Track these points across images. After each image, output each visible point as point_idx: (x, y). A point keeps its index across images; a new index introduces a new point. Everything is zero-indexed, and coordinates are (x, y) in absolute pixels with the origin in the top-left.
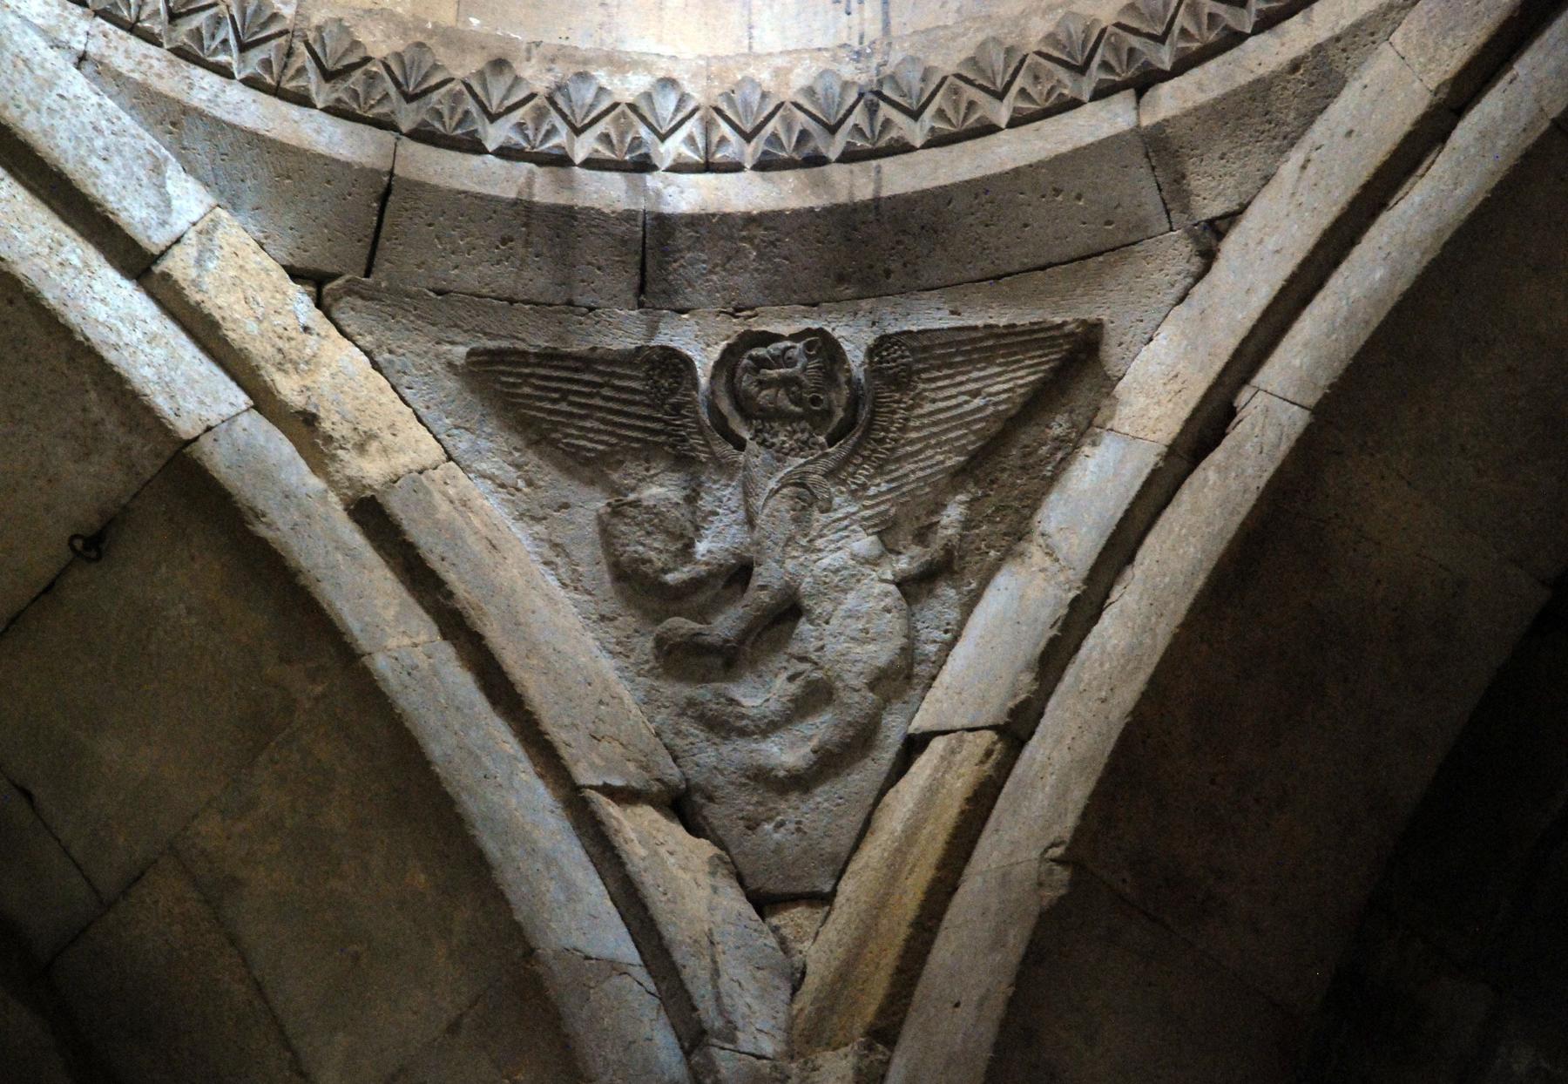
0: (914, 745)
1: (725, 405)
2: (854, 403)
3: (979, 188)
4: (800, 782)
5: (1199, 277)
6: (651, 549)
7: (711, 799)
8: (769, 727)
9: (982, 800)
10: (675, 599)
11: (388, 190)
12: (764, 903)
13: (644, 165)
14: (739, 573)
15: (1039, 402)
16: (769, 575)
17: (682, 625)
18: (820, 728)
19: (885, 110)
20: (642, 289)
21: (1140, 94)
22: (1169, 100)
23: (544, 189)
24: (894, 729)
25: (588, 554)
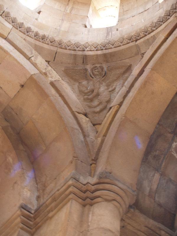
0: (111, 108)
1: (91, 74)
2: (105, 73)
3: (119, 51)
5: (142, 59)
6: (84, 89)
7: (89, 114)
8: (95, 107)
9: (117, 112)
10: (86, 94)
11: (56, 53)
12: (94, 125)
13: (84, 51)
14: (93, 91)
15: (124, 73)
16: (95, 91)
17: (86, 97)
19: (109, 44)
20: (83, 63)
21: (136, 41)
22: (138, 42)
23: (73, 52)
24: (109, 107)
25: (77, 90)
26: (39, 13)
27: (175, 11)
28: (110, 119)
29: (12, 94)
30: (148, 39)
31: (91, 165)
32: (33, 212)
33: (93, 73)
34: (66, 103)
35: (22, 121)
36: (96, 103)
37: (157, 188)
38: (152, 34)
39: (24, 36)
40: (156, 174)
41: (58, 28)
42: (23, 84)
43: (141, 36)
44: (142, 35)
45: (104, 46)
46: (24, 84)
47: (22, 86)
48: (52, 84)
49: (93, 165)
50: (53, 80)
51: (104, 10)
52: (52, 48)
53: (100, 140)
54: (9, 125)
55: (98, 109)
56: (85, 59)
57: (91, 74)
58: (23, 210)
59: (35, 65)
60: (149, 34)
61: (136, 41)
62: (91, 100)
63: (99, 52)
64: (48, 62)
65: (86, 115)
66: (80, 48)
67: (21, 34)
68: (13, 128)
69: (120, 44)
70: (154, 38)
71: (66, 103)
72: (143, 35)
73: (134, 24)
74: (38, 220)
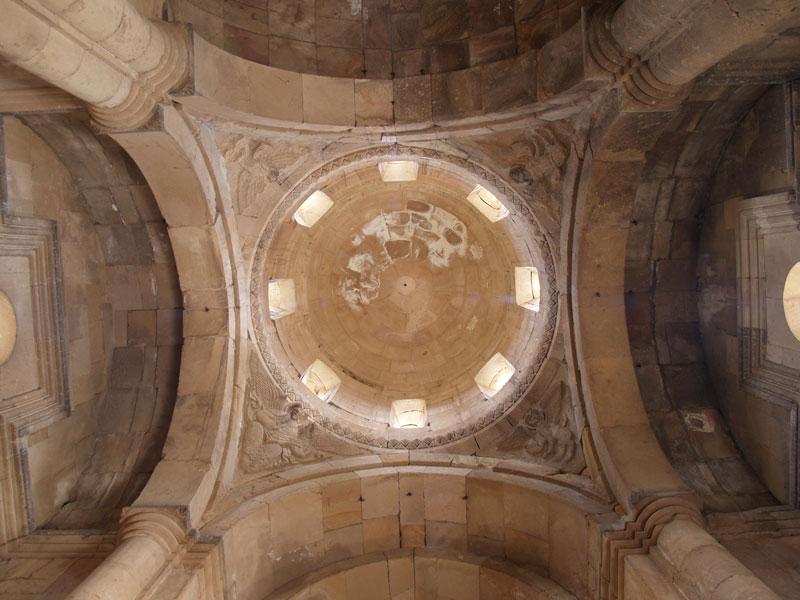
0: (581, 441)
2: (544, 414)
3: (537, 382)
4: (573, 457)
6: (535, 449)
8: (565, 454)
9: (590, 435)
10: (541, 452)
12: (580, 474)
15: (563, 394)
17: (545, 454)
18: (570, 449)
23: (493, 424)
24: (578, 442)
25: (528, 456)
26: (429, 425)
28: (591, 453)
30: (556, 342)
31: (614, 509)
33: (531, 425)
36: (561, 451)
37: (716, 479)
39: (428, 450)
40: (700, 466)
44: (546, 346)
45: (520, 392)
47: (466, 498)
50: (494, 465)
52: (467, 439)
53: (599, 478)
55: (569, 455)
56: (510, 419)
59: (461, 466)
62: (554, 453)
63: (520, 401)
64: (475, 454)
65: (561, 472)
67: (425, 450)
70: (560, 335)
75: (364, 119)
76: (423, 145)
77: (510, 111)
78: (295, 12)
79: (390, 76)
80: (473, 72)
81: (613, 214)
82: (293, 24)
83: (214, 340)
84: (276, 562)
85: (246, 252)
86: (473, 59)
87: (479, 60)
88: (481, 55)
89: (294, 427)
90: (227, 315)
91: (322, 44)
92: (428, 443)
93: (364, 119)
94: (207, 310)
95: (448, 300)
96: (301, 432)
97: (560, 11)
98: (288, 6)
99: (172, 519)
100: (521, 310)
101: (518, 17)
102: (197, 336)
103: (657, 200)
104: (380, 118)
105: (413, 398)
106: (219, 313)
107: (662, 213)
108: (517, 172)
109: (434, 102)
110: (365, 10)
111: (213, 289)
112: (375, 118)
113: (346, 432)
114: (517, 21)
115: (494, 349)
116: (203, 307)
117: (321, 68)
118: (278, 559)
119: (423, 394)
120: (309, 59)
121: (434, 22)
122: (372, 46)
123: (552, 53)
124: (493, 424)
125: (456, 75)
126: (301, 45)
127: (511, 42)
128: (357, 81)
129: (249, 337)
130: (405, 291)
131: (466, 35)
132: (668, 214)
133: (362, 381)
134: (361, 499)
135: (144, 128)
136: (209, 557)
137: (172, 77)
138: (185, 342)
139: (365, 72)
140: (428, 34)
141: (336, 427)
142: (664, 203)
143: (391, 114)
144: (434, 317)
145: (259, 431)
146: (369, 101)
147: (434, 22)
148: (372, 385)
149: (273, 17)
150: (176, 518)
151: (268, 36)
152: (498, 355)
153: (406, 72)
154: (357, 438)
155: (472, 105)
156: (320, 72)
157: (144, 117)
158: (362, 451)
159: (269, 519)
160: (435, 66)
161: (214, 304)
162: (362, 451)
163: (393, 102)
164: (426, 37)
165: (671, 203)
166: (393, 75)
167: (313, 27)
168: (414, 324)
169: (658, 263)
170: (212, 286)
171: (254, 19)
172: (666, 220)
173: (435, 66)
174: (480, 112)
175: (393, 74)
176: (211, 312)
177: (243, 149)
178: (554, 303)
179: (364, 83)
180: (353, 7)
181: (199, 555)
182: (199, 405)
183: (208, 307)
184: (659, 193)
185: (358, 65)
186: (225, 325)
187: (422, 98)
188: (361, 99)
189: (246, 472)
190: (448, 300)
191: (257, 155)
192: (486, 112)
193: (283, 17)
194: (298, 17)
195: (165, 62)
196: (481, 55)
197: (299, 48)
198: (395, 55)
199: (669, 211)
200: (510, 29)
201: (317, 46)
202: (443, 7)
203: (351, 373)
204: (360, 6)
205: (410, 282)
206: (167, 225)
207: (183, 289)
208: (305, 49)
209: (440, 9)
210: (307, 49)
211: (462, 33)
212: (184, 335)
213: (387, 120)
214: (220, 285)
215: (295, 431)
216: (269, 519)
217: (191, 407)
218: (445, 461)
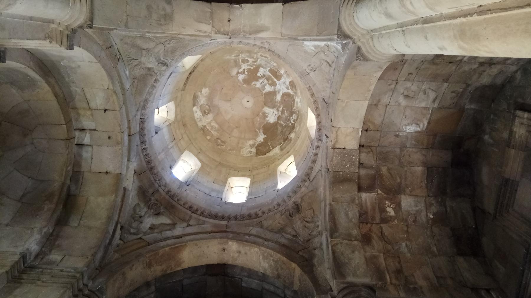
1: (151, 205)
16: (142, 218)
21: (192, 213)
22: (193, 215)
23: (153, 181)
26: (156, 133)
27: (228, 220)
29: (94, 168)
30: (200, 220)
31: (97, 269)
32: (26, 265)
33: (152, 205)
34: (120, 210)
35: (80, 191)
38: (204, 219)
41: (157, 154)
42: (108, 172)
43: (197, 213)
45: (173, 196)
46: (110, 173)
48: (125, 189)
49: (98, 271)
51: (184, 162)
54: (69, 184)
56: (156, 191)
57: (151, 205)
58: (22, 260)
59: (128, 167)
60: (203, 216)
61: (193, 212)
64: (135, 173)
65: (122, 227)
66: (159, 183)
68: (69, 187)
69: (182, 205)
70: (204, 223)
71: (120, 210)
72: (199, 214)
73: (198, 198)
74: (24, 276)
75: (337, 132)
76: (320, 155)
77: (329, 219)
78: (410, 96)
79: (362, 144)
80: (355, 198)
81: (267, 265)
82: (403, 93)
83: (210, 25)
84: (61, 63)
85: (266, 44)
86: (365, 196)
87: (363, 199)
88: (366, 201)
89: (151, 63)
90: (225, 34)
91: (387, 109)
92: (143, 142)
93: (337, 132)
94: (229, 21)
95: (237, 127)
96: (149, 69)
97: (382, 254)
98: (415, 92)
99: (84, 19)
100: (224, 182)
101: (384, 226)
102: (212, 13)
103: (273, 285)
104: (336, 141)
105: (176, 112)
106: (227, 29)
107: (267, 286)
108: (297, 208)
109: (341, 173)
110: (405, 134)
111: (242, 27)
112: (337, 138)
113: (150, 93)
114: (382, 225)
115: (204, 160)
116: (231, 18)
117: (373, 106)
118: (62, 63)
119: (179, 117)
120: (379, 101)
121: (391, 174)
122: (382, 135)
123: (356, 252)
124: (153, 181)
125: (355, 187)
126: (388, 97)
127: (370, 220)
128: (361, 130)
129: (211, 40)
130: (244, 101)
131: (380, 192)
132: (266, 290)
133: (188, 78)
134: (105, 110)
135: (339, 28)
136: (58, 46)
137: (368, 52)
138: (208, 5)
139: (366, 131)
140: (384, 170)
141: (153, 87)
142: (272, 289)
143: (338, 147)
144: (228, 117)
145: (151, 45)
146: (347, 135)
147: (391, 174)
148: (185, 84)
149: (409, 84)
150: (83, 22)
151: (397, 80)
152: (199, 164)
153: (363, 156)
154: (146, 101)
155: (336, 196)
156: (370, 107)
157: (346, 28)
158: (138, 105)
159: (89, 62)
160: (363, 172)
161: (233, 26)
162: (138, 105)
163: (344, 149)
164: (382, 168)
165: (271, 292)
166: (361, 146)
167: (399, 104)
168: (223, 106)
169: (240, 280)
170: (244, 26)
171: (409, 74)
172: (263, 288)
173: (363, 172)
174: (332, 200)
175: (363, 146)
176: (227, 23)
177: (328, 56)
178: (223, 218)
179: (359, 133)
180: (408, 127)
181: (59, 40)
182: (165, 15)
183: (231, 22)
184: (278, 288)
185: (371, 127)
186: (218, 32)
187: (345, 166)
188: (349, 131)
189: (121, 40)
190: (237, 127)
191: (325, 64)
192: (330, 205)
193: (406, 89)
194: (407, 97)
195: (377, 52)
196: (366, 201)
197: (387, 96)
198: (374, 148)
199: (267, 290)
200: (378, 220)
201: (386, 106)
202: (399, 180)
203: (193, 71)
204: (408, 131)
205: (249, 105)
206: (285, 4)
207: (243, 5)
208: (385, 100)
209: (398, 178)
210: (385, 100)
211: (381, 190)
212: (213, 4)
213: (334, 144)
214: (244, 32)
215: (150, 66)
216: (89, 62)
217: (164, 9)
218: (131, 157)
